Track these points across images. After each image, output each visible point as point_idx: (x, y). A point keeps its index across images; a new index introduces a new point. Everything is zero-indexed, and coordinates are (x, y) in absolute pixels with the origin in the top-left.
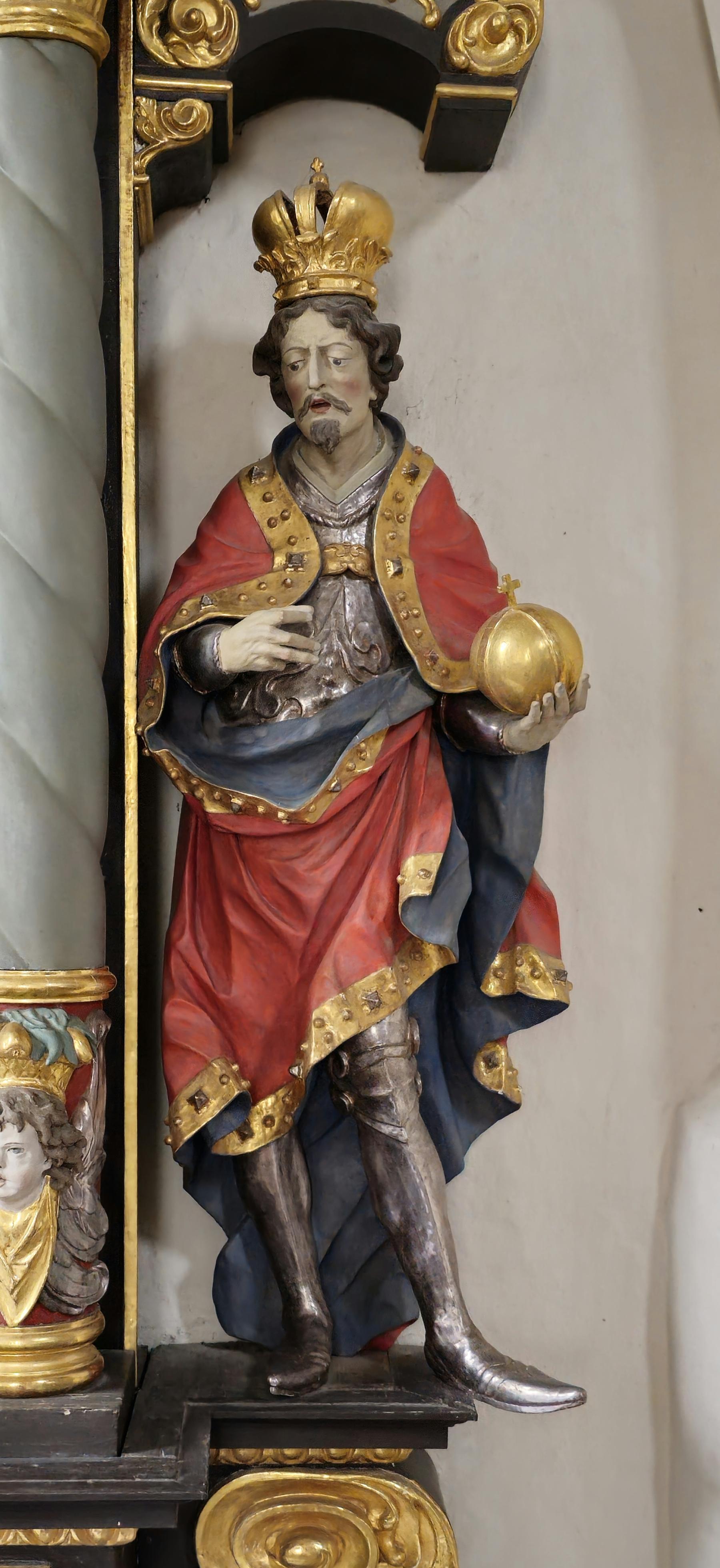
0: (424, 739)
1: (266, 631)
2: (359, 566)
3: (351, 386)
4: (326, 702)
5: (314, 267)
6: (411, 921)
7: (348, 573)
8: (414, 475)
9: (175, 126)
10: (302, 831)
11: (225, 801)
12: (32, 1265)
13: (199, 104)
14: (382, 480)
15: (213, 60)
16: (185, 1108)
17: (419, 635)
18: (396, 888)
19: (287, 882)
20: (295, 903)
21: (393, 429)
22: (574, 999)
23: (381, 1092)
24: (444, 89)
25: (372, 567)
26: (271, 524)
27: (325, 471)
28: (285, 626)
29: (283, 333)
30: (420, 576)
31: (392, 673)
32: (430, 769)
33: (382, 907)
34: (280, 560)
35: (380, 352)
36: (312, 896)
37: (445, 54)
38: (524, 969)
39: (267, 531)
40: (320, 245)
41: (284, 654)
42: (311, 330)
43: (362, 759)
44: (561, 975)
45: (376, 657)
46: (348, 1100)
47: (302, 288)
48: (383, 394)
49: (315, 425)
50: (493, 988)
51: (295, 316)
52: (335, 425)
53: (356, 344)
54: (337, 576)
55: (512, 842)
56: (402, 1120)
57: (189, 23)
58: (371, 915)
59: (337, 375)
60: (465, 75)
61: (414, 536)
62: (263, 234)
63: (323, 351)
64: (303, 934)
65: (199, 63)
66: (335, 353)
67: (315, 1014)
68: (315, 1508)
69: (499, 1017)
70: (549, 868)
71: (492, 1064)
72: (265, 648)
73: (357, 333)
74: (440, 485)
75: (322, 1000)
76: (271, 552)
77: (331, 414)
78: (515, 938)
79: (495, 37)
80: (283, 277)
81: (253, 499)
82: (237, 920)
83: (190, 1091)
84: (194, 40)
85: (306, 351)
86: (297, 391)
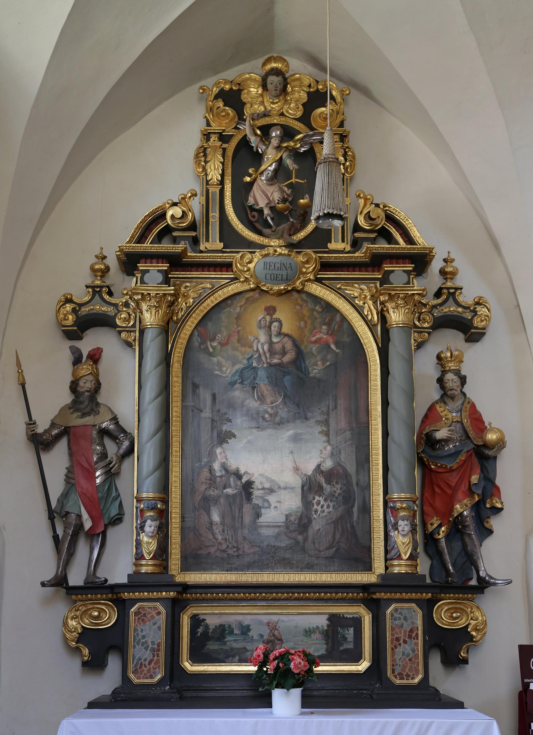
0: (473, 454)
1: (446, 431)
2: (459, 420)
3: (458, 386)
4: (455, 446)
5: (450, 365)
6: (473, 489)
7: (458, 421)
8: (469, 403)
9: (421, 338)
10: (451, 470)
11: (436, 465)
12: (409, 548)
13: (427, 334)
14: (463, 404)
15: (428, 326)
16: (429, 526)
17: (472, 434)
18: (470, 482)
19: (447, 482)
20: (449, 486)
21: (464, 394)
22: (504, 508)
23: (467, 523)
24: (472, 331)
25: (462, 420)
26: (442, 412)
27: (452, 402)
28: (449, 431)
29: (444, 376)
30: (471, 422)
31: (467, 441)
32: (475, 460)
33: (467, 486)
34: (444, 419)
35: (463, 380)
36: (453, 484)
37: (472, 324)
38: (494, 501)
39: (441, 414)
40: (451, 361)
41: (449, 436)
42: (450, 376)
43: (462, 457)
44: (502, 503)
45: (464, 438)
46: (460, 527)
47: (448, 369)
48: (463, 387)
49: (451, 394)
50: (488, 506)
51: (447, 373)
52: (455, 394)
53: (459, 379)
54: (455, 422)
55: (491, 476)
56: (472, 531)
57: (424, 319)
58: (465, 487)
59: (455, 384)
60: (476, 328)
61: (469, 415)
62: (439, 357)
63: (452, 380)
64: (451, 492)
65: (425, 326)
66: (455, 380)
67: (455, 507)
68: (458, 606)
69: (489, 512)
70: (498, 482)
71: (487, 522)
72: (446, 435)
73: (459, 377)
74: (473, 406)
75: (456, 505)
76: (442, 418)
77: (454, 392)
78: (492, 496)
79: (482, 321)
80: (442, 366)
81: (438, 408)
82: (437, 490)
83: (430, 522)
84: (424, 323)
85: (449, 380)
86: (447, 387)
